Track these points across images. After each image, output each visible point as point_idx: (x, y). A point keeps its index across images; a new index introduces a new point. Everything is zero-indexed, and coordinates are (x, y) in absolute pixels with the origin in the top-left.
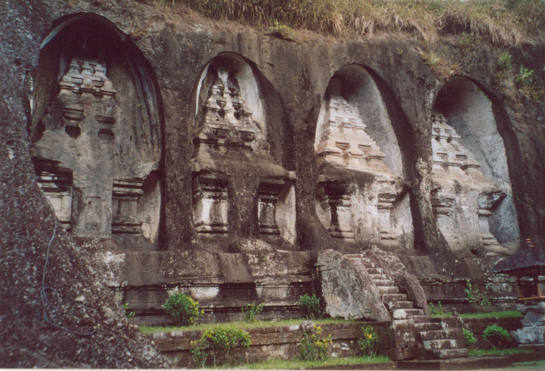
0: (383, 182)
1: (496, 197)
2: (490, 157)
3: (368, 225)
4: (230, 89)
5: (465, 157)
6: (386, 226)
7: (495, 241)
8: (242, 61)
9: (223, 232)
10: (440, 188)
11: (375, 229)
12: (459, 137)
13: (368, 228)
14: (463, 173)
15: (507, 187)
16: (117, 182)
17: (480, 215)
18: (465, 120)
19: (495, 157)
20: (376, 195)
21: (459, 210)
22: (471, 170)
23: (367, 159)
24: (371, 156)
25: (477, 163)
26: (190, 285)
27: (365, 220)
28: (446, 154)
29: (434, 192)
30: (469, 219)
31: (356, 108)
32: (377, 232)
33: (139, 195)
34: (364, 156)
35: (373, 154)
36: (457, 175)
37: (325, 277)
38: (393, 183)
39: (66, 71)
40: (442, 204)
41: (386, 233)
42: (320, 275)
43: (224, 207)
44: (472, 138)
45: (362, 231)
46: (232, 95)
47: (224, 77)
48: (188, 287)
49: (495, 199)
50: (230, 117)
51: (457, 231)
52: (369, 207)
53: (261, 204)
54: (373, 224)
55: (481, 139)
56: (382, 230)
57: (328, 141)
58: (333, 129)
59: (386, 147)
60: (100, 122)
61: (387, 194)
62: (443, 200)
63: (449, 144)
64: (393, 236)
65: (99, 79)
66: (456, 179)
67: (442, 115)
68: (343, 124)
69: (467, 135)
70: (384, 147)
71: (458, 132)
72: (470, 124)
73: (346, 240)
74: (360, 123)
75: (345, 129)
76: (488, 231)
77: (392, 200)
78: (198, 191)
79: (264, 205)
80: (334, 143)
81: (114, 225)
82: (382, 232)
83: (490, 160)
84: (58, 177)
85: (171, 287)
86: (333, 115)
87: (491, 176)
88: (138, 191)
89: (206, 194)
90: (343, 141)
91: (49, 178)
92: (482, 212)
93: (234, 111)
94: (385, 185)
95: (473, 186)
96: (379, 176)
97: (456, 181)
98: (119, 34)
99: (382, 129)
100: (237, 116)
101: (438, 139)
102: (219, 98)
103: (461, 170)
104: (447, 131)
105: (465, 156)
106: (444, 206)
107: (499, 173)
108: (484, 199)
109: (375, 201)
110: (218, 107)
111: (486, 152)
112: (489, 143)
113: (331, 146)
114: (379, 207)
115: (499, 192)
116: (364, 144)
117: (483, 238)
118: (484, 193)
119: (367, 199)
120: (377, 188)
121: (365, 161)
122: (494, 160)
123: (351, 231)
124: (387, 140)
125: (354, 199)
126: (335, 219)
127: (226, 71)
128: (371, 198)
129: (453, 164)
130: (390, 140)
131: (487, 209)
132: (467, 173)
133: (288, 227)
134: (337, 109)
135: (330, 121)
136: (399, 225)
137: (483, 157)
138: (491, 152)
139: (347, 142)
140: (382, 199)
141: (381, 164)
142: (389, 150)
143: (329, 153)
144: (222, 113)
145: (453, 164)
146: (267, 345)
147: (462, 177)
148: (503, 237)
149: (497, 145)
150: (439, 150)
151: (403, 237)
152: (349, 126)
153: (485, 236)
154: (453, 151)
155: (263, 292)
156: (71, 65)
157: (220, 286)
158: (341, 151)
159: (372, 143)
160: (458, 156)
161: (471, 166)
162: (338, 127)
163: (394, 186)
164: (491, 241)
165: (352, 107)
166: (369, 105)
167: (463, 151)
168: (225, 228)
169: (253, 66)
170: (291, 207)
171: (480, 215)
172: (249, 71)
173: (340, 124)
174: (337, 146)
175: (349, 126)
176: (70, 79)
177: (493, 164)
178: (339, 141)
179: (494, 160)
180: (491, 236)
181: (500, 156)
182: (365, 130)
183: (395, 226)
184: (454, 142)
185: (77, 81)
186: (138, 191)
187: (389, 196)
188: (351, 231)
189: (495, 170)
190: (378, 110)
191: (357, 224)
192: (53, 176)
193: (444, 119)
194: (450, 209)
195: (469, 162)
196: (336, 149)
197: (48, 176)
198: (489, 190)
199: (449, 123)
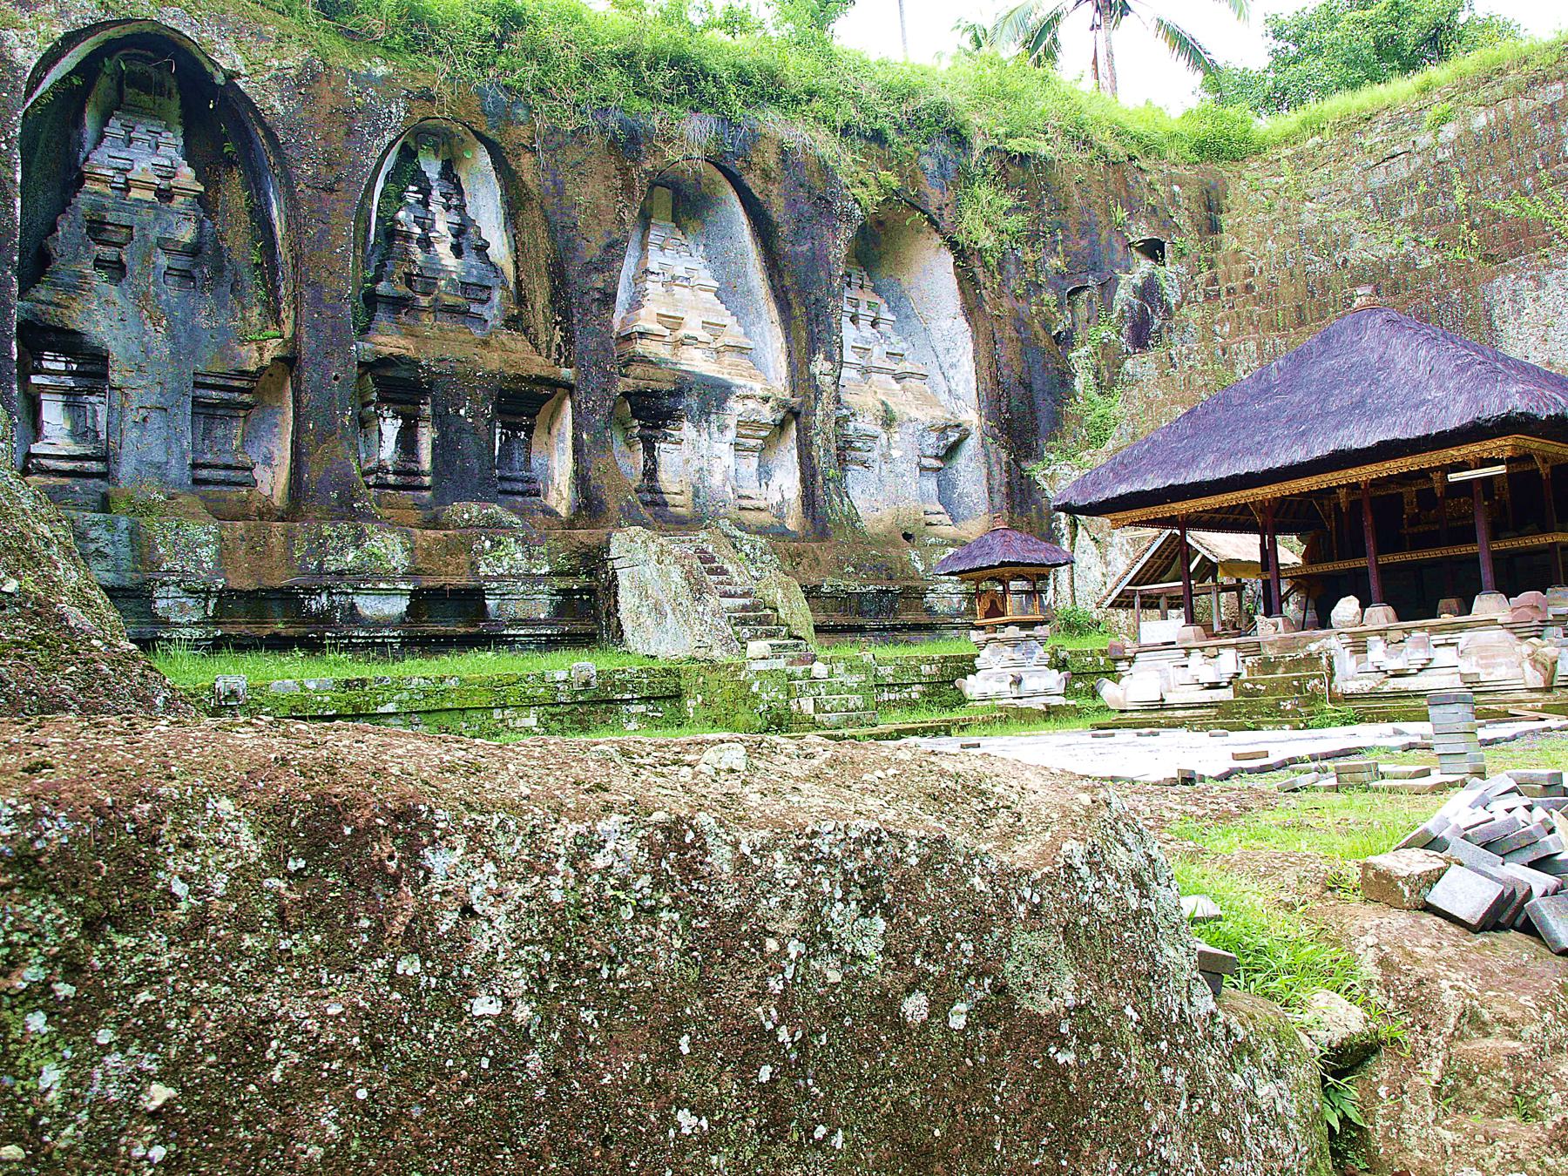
0: (747, 397)
1: (953, 437)
2: (946, 361)
3: (716, 480)
6: (751, 487)
7: (946, 519)
9: (422, 488)
10: (853, 415)
12: (894, 318)
13: (714, 487)
15: (971, 417)
16: (200, 379)
17: (923, 469)
18: (905, 285)
19: (954, 360)
20: (732, 422)
21: (886, 458)
22: (910, 383)
26: (350, 591)
27: (709, 471)
29: (841, 422)
30: (903, 476)
31: (702, 248)
32: (732, 496)
33: (247, 407)
36: (888, 392)
37: (623, 581)
38: (766, 400)
40: (858, 445)
42: (615, 578)
43: (426, 437)
44: (915, 321)
45: (702, 494)
47: (431, 167)
49: (952, 440)
51: (880, 498)
52: (718, 445)
53: (502, 433)
55: (933, 325)
57: (642, 312)
58: (653, 287)
63: (874, 331)
64: (762, 504)
65: (167, 163)
66: (884, 399)
69: (907, 317)
71: (891, 309)
72: (914, 294)
73: (672, 509)
74: (705, 277)
75: (675, 288)
76: (935, 498)
77: (763, 434)
78: (371, 403)
79: (506, 435)
80: (655, 318)
81: (195, 466)
83: (945, 366)
84: (79, 364)
86: (655, 261)
87: (946, 396)
88: (246, 398)
91: (61, 366)
92: (926, 462)
93: (451, 239)
94: (751, 404)
95: (914, 414)
96: (739, 387)
97: (883, 403)
98: (209, 68)
101: (854, 319)
102: (420, 212)
103: (893, 382)
106: (859, 449)
107: (961, 390)
108: (932, 438)
109: (730, 435)
110: (417, 230)
111: (939, 349)
112: (946, 333)
113: (646, 320)
114: (738, 447)
115: (958, 426)
117: (926, 513)
118: (932, 428)
119: (714, 429)
120: (735, 407)
121: (715, 355)
122: (952, 366)
124: (759, 316)
125: (687, 430)
128: (722, 429)
129: (880, 370)
131: (937, 457)
132: (904, 389)
133: (556, 481)
134: (662, 249)
135: (647, 271)
136: (773, 485)
137: (935, 359)
141: (746, 363)
143: (642, 335)
145: (880, 370)
147: (894, 395)
148: (961, 510)
149: (959, 337)
151: (780, 507)
152: (685, 283)
153: (928, 508)
154: (880, 345)
156: (105, 129)
157: (413, 594)
158: (667, 332)
159: (730, 321)
164: (939, 517)
166: (727, 243)
168: (427, 480)
170: (562, 442)
171: (923, 469)
175: (685, 283)
176: (107, 160)
177: (951, 373)
179: (952, 366)
180: (940, 508)
181: (964, 358)
184: (882, 327)
185: (120, 163)
186: (246, 398)
187: (757, 425)
189: (953, 386)
192: (67, 362)
194: (870, 454)
195: (906, 366)
196: (656, 328)
198: (941, 423)
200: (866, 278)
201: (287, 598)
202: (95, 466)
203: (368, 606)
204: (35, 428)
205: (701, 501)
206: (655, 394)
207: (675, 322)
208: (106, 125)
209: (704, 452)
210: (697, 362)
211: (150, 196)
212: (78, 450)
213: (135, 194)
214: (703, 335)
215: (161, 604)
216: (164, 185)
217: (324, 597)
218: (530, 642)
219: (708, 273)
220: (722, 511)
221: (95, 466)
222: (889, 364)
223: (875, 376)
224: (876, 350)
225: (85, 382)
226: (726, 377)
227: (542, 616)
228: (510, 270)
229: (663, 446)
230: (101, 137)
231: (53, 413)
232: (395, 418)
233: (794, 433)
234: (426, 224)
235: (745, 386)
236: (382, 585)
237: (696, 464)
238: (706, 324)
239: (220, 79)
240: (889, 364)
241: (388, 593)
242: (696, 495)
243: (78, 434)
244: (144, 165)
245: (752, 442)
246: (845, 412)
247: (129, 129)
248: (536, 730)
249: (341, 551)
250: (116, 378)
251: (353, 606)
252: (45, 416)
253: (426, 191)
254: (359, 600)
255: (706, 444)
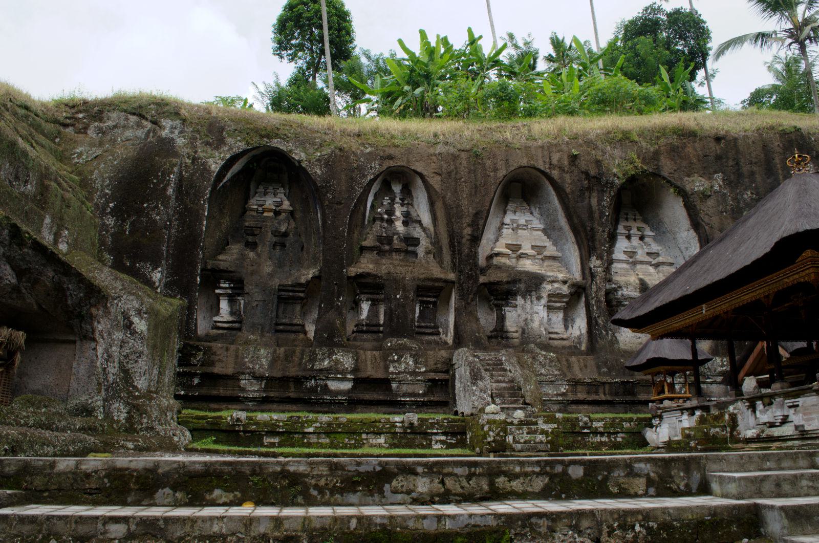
3: (536, 324)
4: (400, 199)
5: (657, 254)
8: (412, 173)
9: (379, 332)
11: (543, 329)
14: (651, 269)
16: (281, 288)
20: (545, 295)
22: (661, 268)
23: (542, 260)
24: (546, 257)
25: (671, 261)
27: (531, 320)
28: (636, 252)
34: (540, 257)
35: (546, 253)
38: (565, 282)
39: (254, 196)
41: (557, 333)
43: (382, 310)
44: (668, 235)
45: (527, 331)
46: (402, 205)
47: (397, 189)
48: (324, 380)
50: (399, 226)
54: (541, 324)
55: (678, 236)
56: (551, 330)
58: (506, 231)
59: (566, 247)
60: (275, 236)
61: (558, 294)
62: (626, 299)
63: (641, 242)
64: (565, 336)
67: (637, 212)
68: (518, 226)
69: (664, 233)
70: (565, 247)
72: (666, 220)
74: (537, 223)
75: (520, 231)
77: (565, 300)
80: (504, 246)
82: (550, 333)
85: (308, 379)
88: (302, 295)
89: (363, 297)
90: (515, 243)
91: (227, 285)
93: (402, 218)
94: (556, 285)
96: (549, 277)
97: (641, 280)
99: (561, 229)
100: (405, 223)
101: (629, 237)
104: (639, 229)
105: (658, 253)
109: (544, 301)
113: (501, 248)
114: (549, 308)
116: (539, 244)
119: (534, 298)
120: (547, 288)
123: (517, 332)
124: (567, 240)
125: (520, 301)
126: (501, 319)
127: (400, 182)
128: (539, 298)
129: (642, 263)
130: (570, 240)
135: (503, 224)
136: (576, 326)
138: (687, 249)
139: (519, 243)
140: (553, 299)
141: (556, 264)
142: (569, 249)
143: (498, 255)
144: (390, 222)
145: (642, 263)
146: (367, 433)
147: (650, 275)
150: (626, 248)
151: (579, 337)
155: (398, 387)
157: (355, 380)
158: (510, 252)
159: (548, 243)
160: (648, 254)
161: (663, 263)
162: (513, 229)
163: (566, 286)
165: (533, 209)
166: (548, 205)
167: (655, 247)
168: (381, 328)
169: (421, 176)
172: (419, 182)
173: (515, 225)
174: (508, 248)
178: (510, 242)
182: (544, 231)
183: (572, 327)
184: (647, 240)
186: (302, 295)
188: (517, 332)
190: (556, 210)
191: (522, 324)
193: (638, 217)
195: (660, 259)
197: (225, 283)
199: (645, 221)
200: (638, 214)
201: (298, 381)
202: (237, 325)
203: (333, 385)
204: (217, 311)
205: (526, 335)
206: (498, 283)
207: (515, 248)
208: (258, 188)
209: (528, 310)
210: (528, 265)
211: (271, 214)
212: (230, 319)
213: (265, 214)
214: (531, 252)
215: (243, 382)
216: (278, 209)
217: (313, 382)
218: (413, 405)
219: (538, 221)
220: (538, 340)
221: (237, 325)
222: (648, 259)
223: (638, 266)
224: (640, 252)
225: (237, 291)
226: (543, 272)
227: (421, 392)
228: (432, 229)
229: (507, 308)
230: (256, 193)
231: (224, 305)
232: (367, 300)
233: (583, 299)
234: (391, 212)
235: (552, 276)
236: (339, 376)
237: (524, 317)
238: (533, 247)
239: (297, 164)
240: (648, 259)
241: (344, 379)
242: (523, 332)
243: (232, 313)
244: (269, 202)
245: (558, 305)
246: (614, 286)
247: (266, 189)
248: (384, 445)
249: (322, 360)
250: (247, 290)
251: (326, 385)
252: (221, 306)
253: (393, 200)
254: (329, 383)
255: (529, 307)
